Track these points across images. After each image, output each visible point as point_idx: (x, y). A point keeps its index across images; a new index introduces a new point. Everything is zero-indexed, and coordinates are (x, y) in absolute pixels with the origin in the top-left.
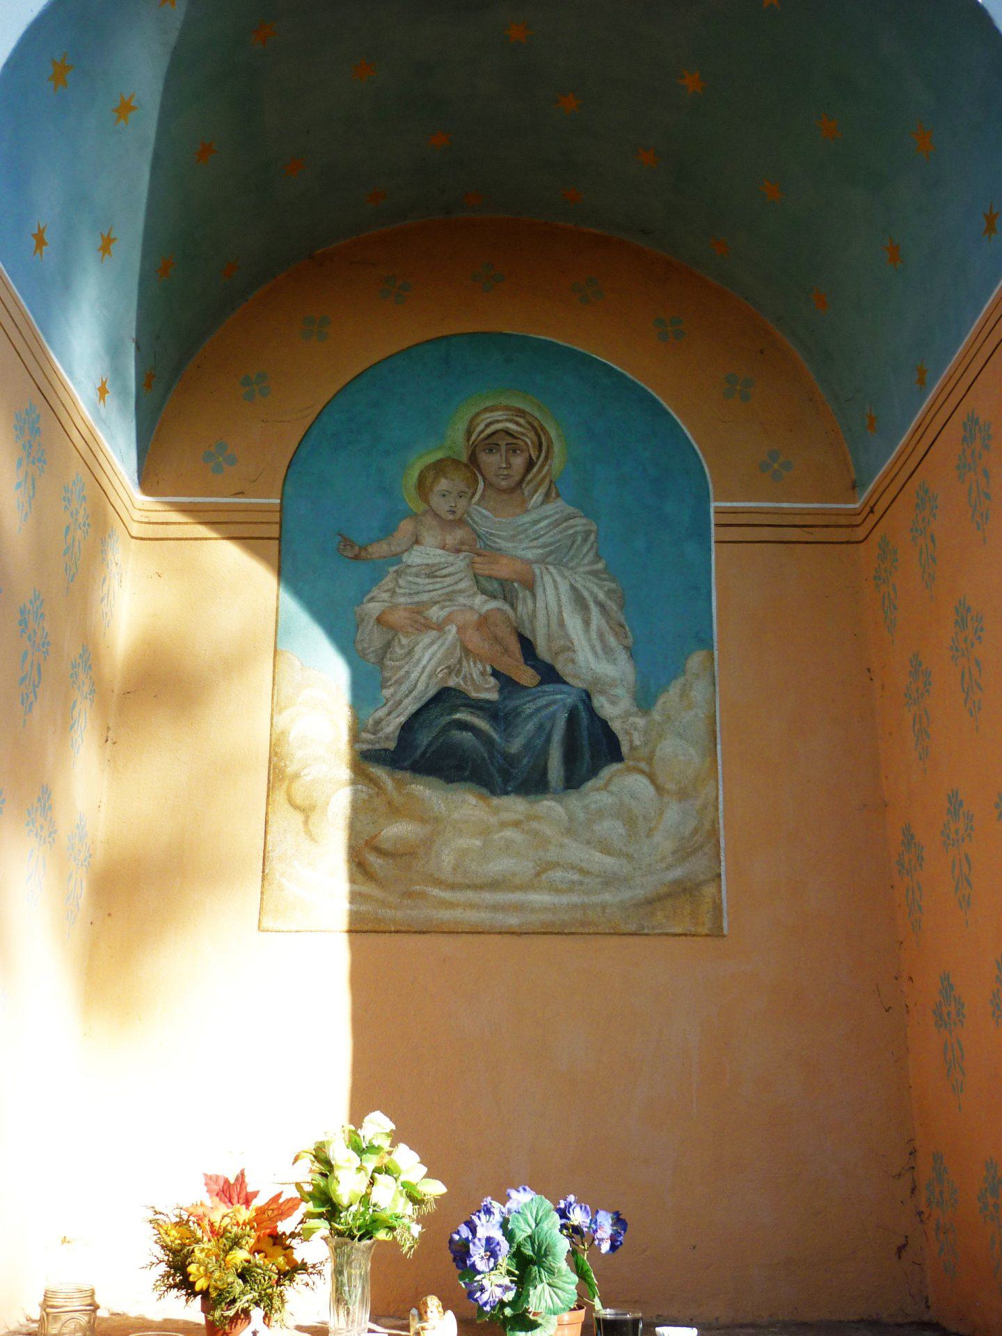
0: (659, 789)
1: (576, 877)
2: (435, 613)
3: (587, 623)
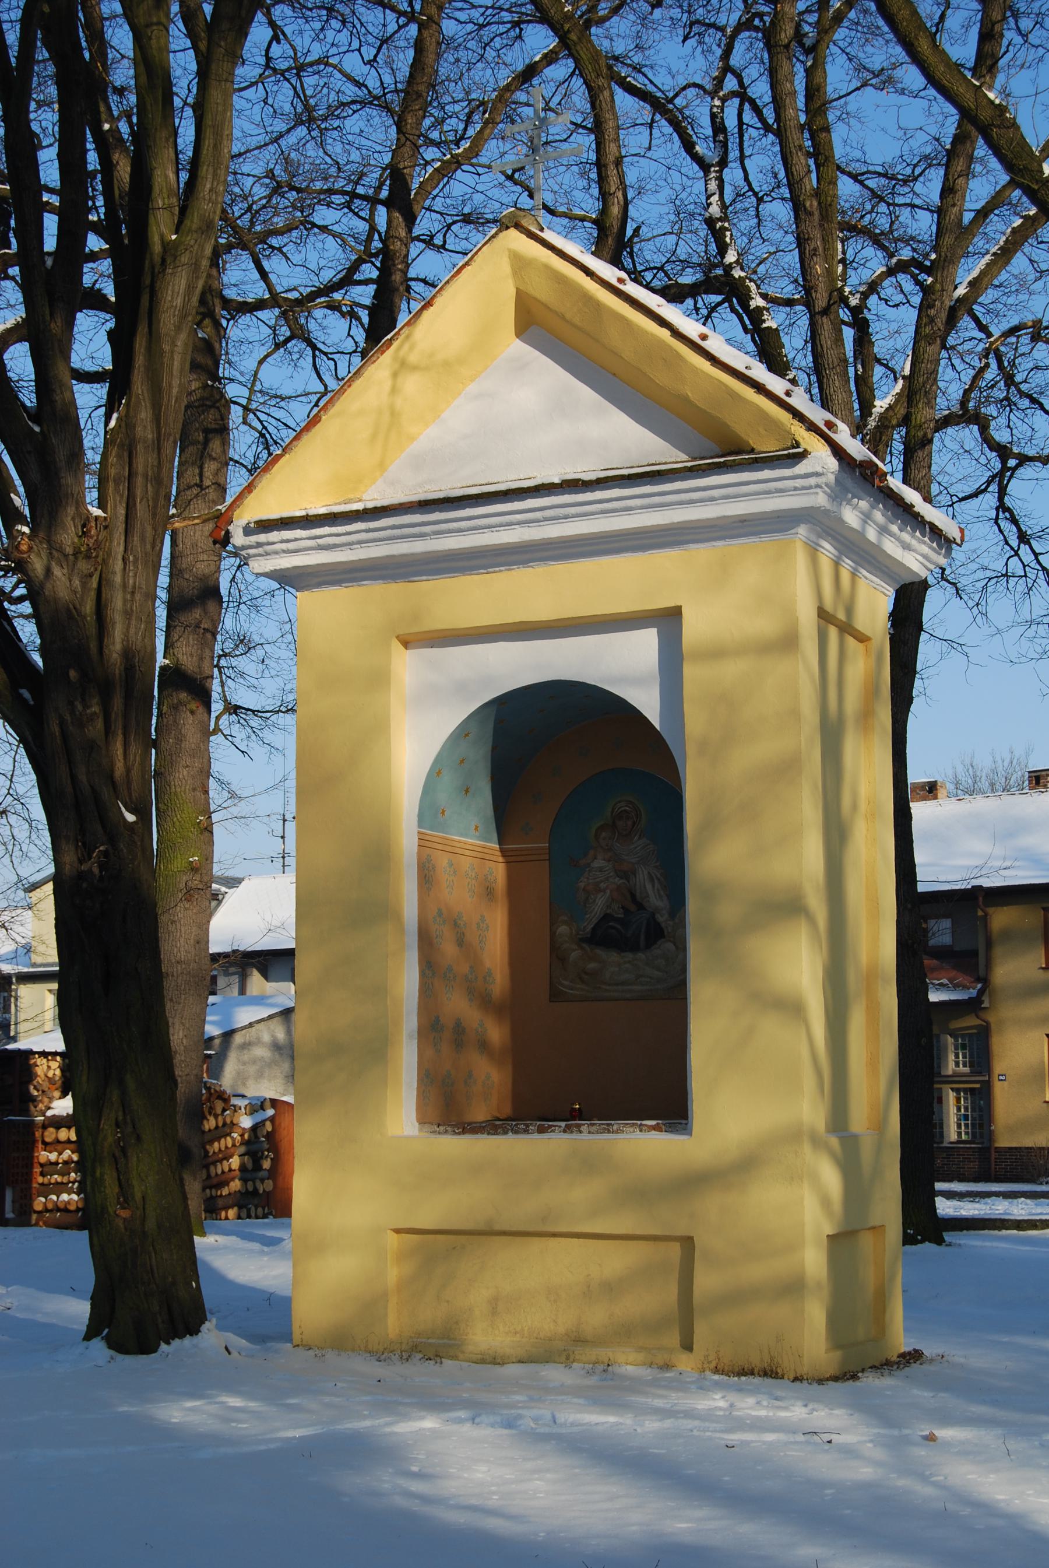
0: (677, 948)
1: (649, 980)
2: (603, 885)
3: (653, 886)
